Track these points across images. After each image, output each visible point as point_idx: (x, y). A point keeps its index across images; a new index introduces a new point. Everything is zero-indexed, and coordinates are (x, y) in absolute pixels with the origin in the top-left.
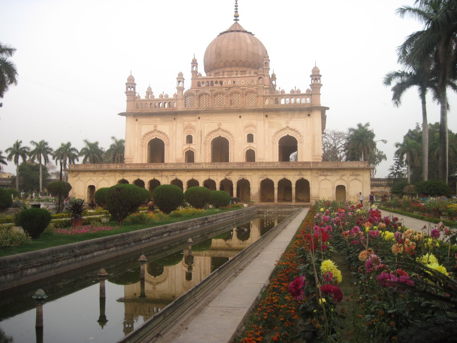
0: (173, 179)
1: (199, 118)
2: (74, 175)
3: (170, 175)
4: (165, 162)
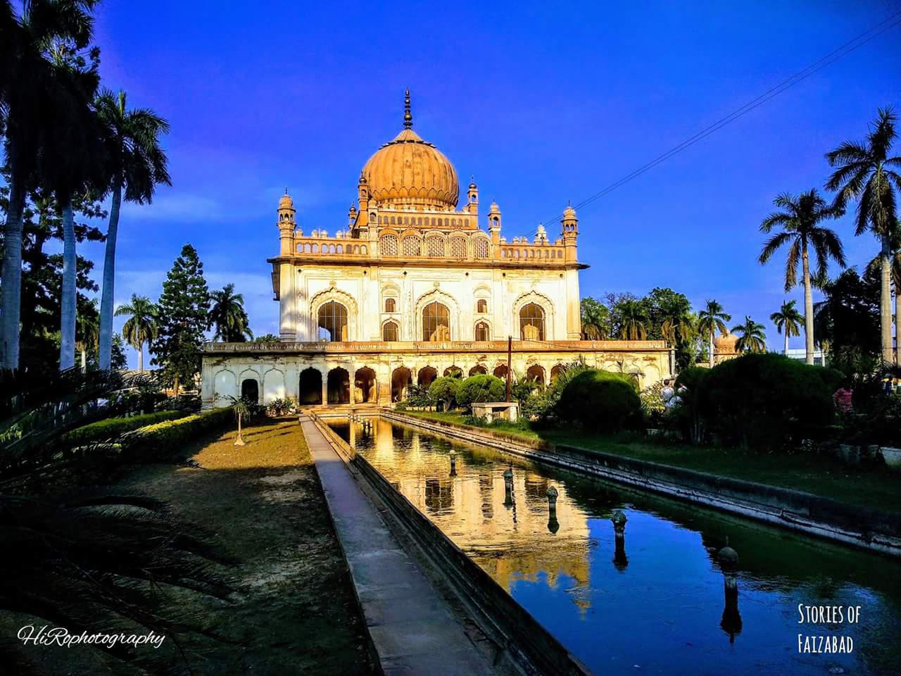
0: (396, 367)
2: (215, 362)
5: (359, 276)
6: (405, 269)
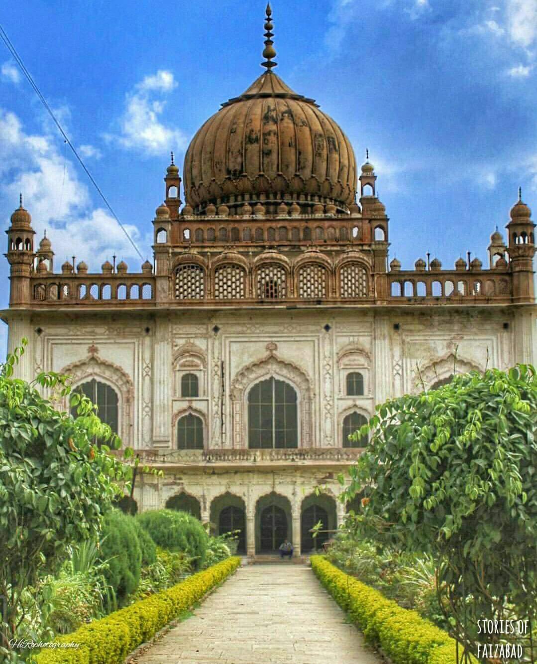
1: (216, 329)
3: (166, 481)
4: (205, 447)
5: (137, 335)
6: (215, 322)
